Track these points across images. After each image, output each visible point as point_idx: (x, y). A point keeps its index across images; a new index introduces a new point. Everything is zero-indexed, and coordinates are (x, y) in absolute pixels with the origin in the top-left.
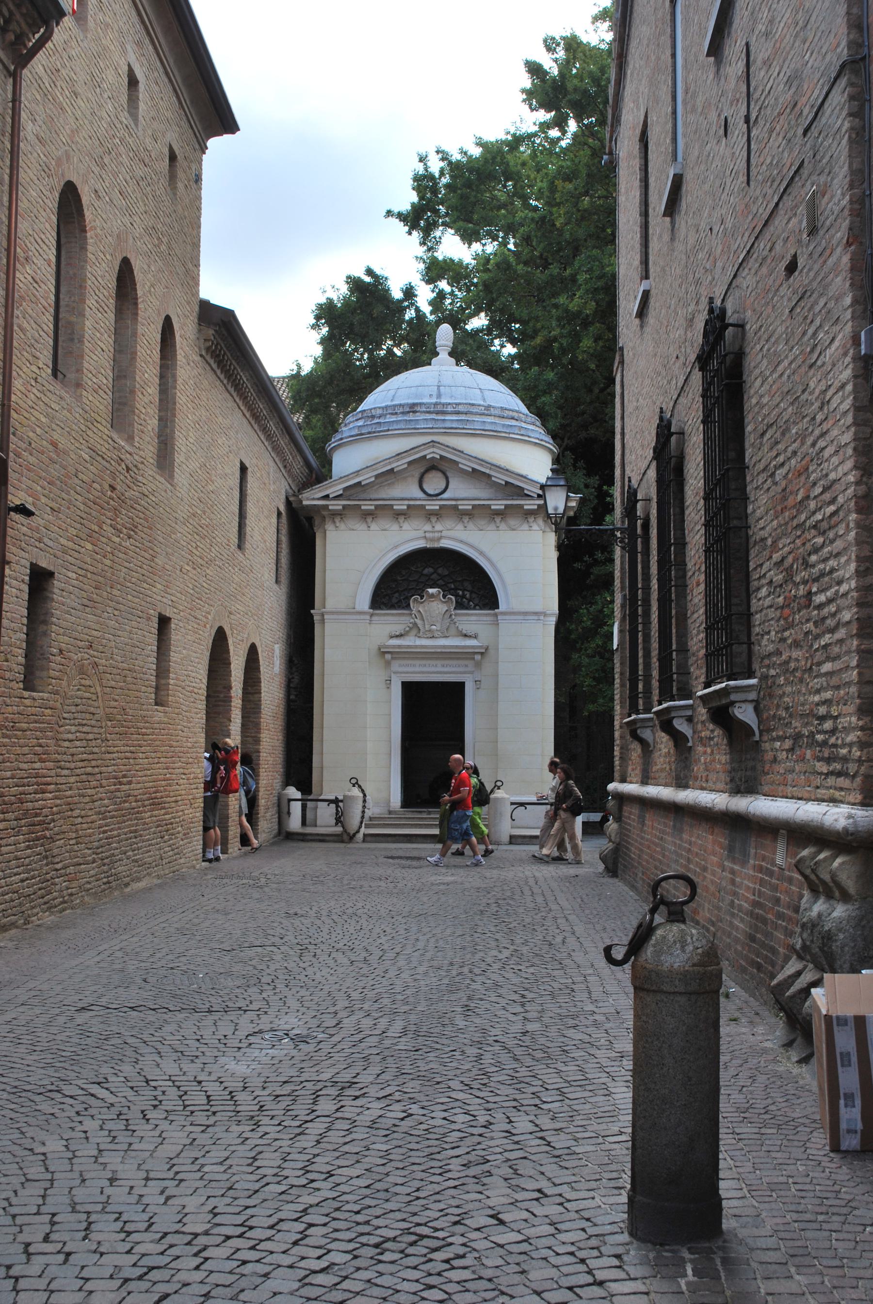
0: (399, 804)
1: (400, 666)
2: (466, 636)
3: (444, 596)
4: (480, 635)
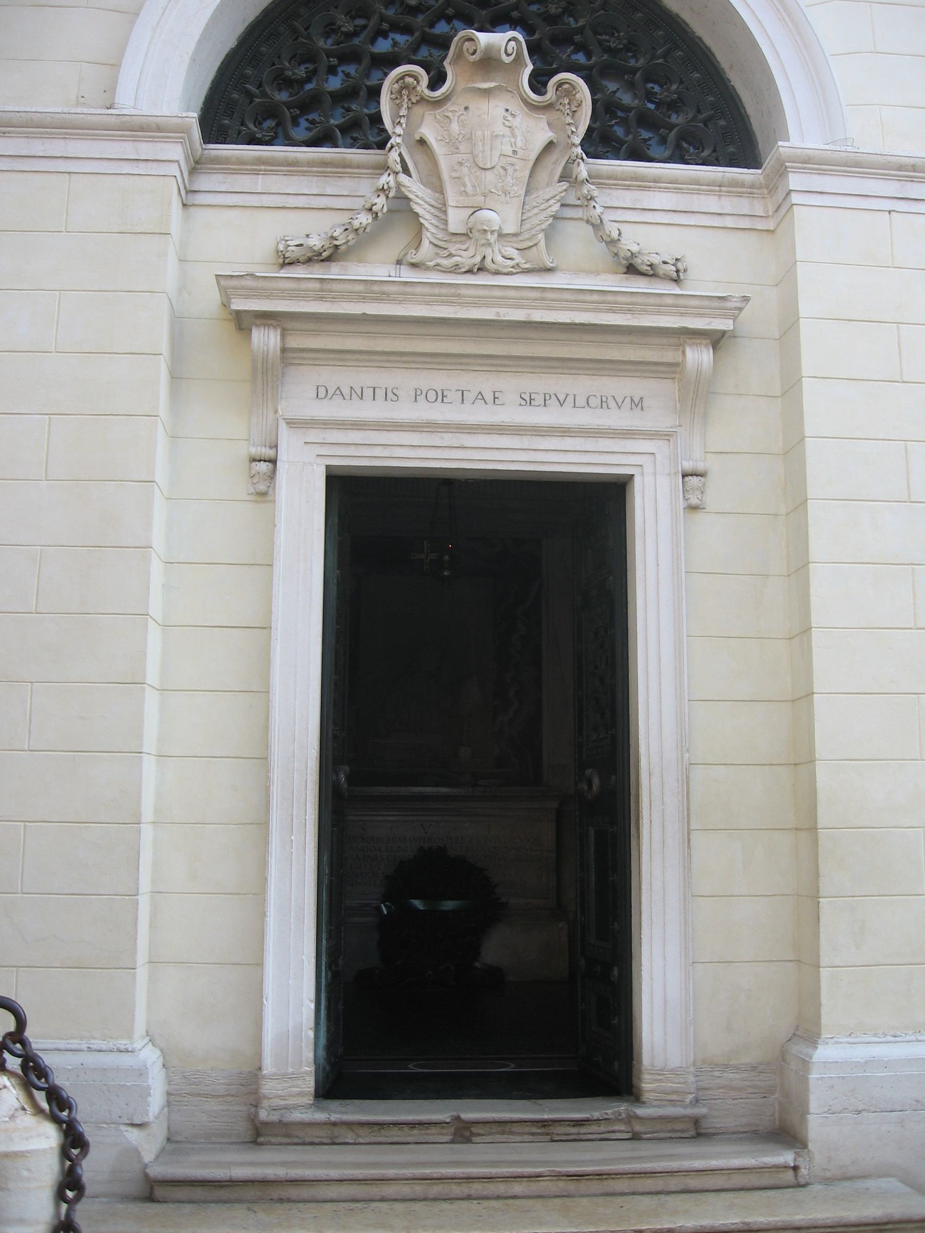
0: (309, 1084)
1: (322, 394)
2: (632, 269)
3: (538, 83)
4: (691, 274)
